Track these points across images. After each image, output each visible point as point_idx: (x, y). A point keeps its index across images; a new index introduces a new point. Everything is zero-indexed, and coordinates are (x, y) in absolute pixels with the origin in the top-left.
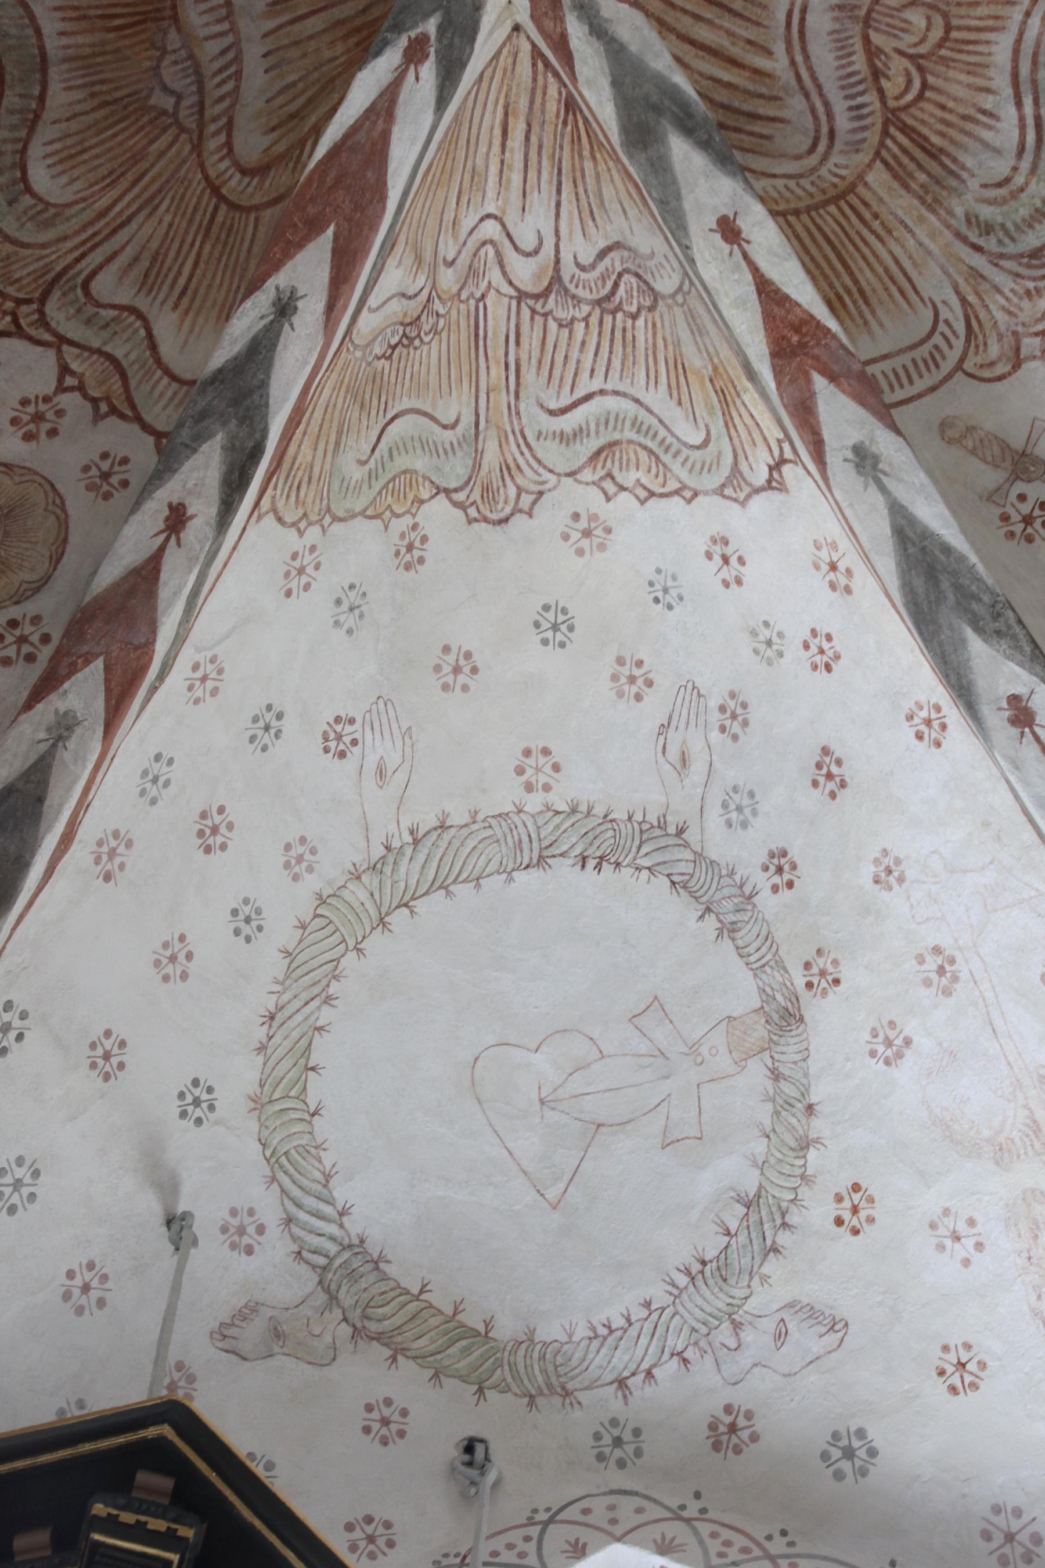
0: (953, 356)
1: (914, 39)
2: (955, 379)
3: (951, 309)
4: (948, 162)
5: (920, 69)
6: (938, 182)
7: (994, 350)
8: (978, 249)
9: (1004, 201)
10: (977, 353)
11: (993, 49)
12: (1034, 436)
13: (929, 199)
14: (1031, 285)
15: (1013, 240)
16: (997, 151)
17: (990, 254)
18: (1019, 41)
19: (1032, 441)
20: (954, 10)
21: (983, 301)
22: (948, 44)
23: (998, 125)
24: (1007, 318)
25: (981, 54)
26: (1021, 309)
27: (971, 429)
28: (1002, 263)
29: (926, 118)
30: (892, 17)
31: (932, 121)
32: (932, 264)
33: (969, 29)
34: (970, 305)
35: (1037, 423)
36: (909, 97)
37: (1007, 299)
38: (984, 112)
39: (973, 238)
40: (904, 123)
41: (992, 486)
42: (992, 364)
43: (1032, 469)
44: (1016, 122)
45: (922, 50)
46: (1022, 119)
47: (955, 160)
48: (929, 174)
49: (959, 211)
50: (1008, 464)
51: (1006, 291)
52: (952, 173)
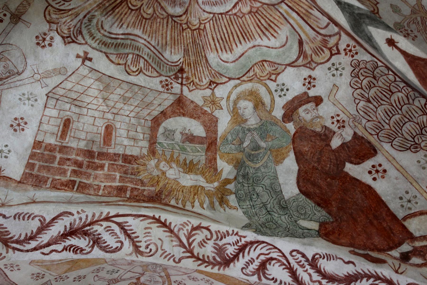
0: (53, 4)
1: (145, 9)
2: (46, 3)
3: (68, 6)
4: (110, 13)
5: (137, 10)
6: (105, 9)
7: (54, 16)
8: (85, 17)
9: (97, 26)
10: (54, 11)
11: (138, 30)
12: (25, 23)
13: (101, 6)
14: (72, 30)
15: (86, 27)
16: (111, 27)
17: (83, 20)
18: (139, 37)
19: (24, 22)
20: (150, 21)
21: (69, 16)
22: (142, 18)
23: (118, 28)
24: (63, 22)
25: (138, 26)
26: (65, 26)
27: (29, 4)
28: (80, 23)
29: (123, 9)
30: (152, 4)
31: (122, 10)
32: (82, 3)
33: (145, 24)
34: (69, 12)
35: (29, 24)
36: (130, 5)
37: (69, 23)
38: (122, 25)
39: (88, 16)
40: (123, 2)
41: (9, 7)
42: (50, 15)
43: (14, 20)
44: (118, 33)
45: (142, 11)
46: (118, 34)
47: (110, 15)
48: (108, 7)
49: (96, 13)
50: (17, 13)
51: (71, 23)
52: (107, 13)
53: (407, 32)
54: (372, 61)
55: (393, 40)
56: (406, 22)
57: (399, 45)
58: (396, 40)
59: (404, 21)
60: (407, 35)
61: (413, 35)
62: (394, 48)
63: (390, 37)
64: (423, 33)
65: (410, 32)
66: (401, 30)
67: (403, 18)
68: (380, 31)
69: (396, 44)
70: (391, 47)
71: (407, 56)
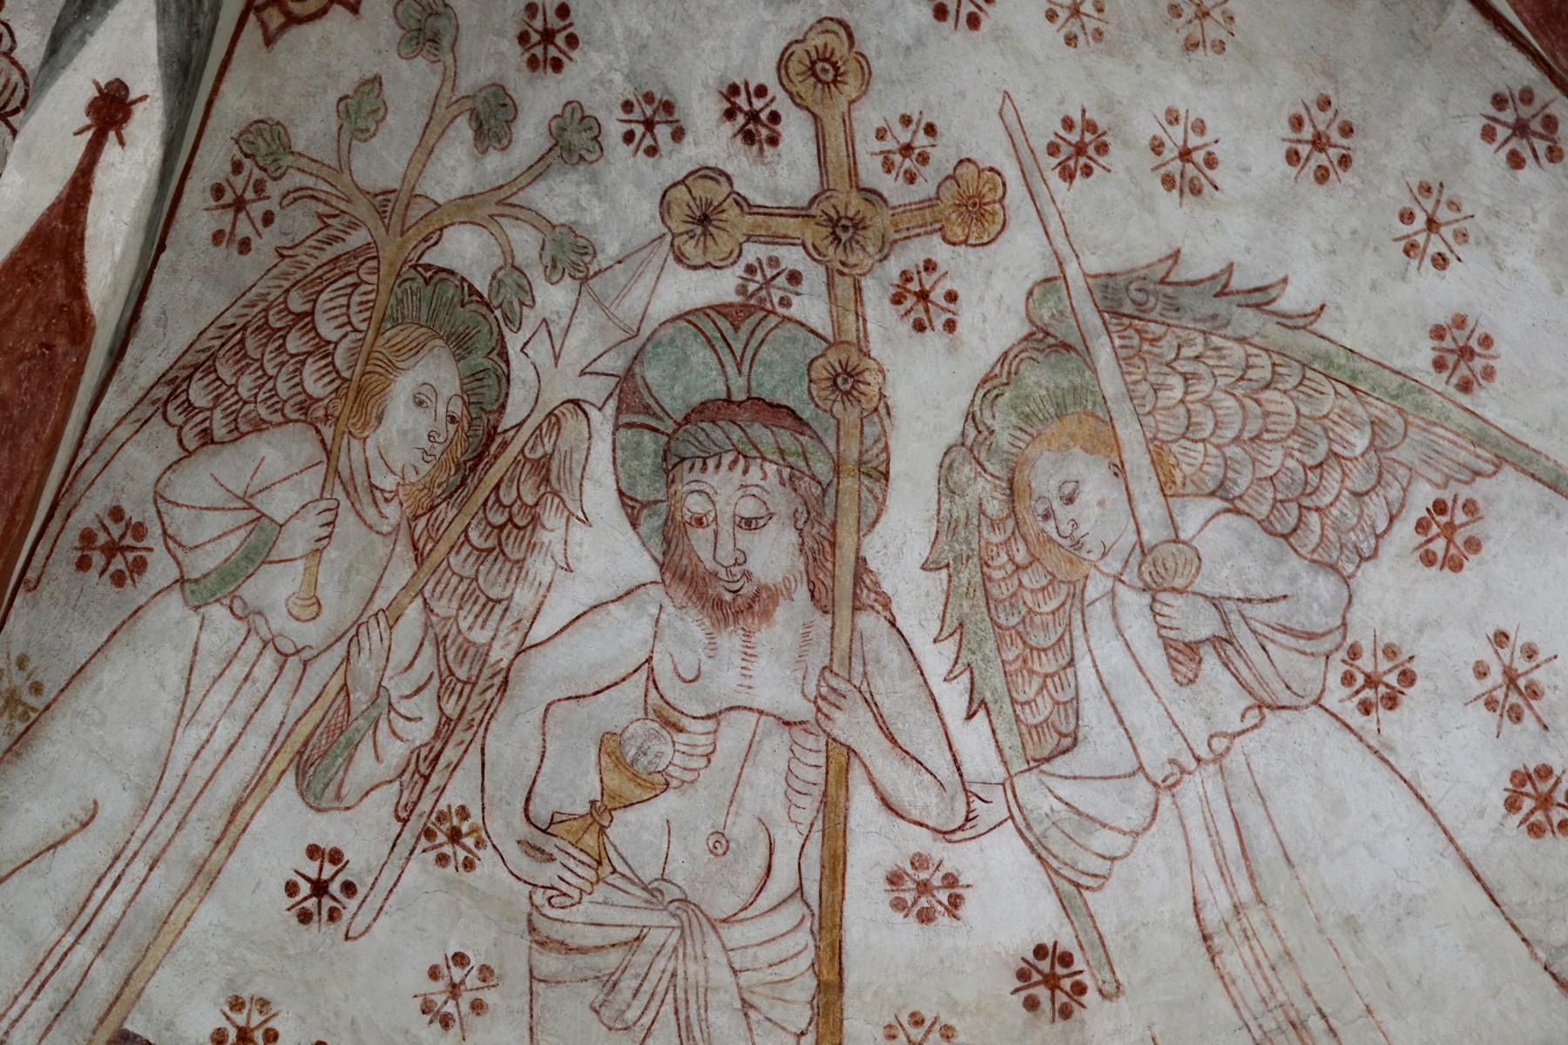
53: (250, 195)
54: (24, 75)
55: (127, 115)
56: (310, 181)
57: (111, 150)
58: (132, 129)
59: (314, 167)
60: (228, 197)
61: (244, 229)
62: (89, 134)
63: (133, 96)
64: (285, 275)
65: (257, 210)
66: (248, 163)
67: (330, 158)
68: (150, 34)
69: (112, 134)
70: (88, 121)
71: (67, 209)
